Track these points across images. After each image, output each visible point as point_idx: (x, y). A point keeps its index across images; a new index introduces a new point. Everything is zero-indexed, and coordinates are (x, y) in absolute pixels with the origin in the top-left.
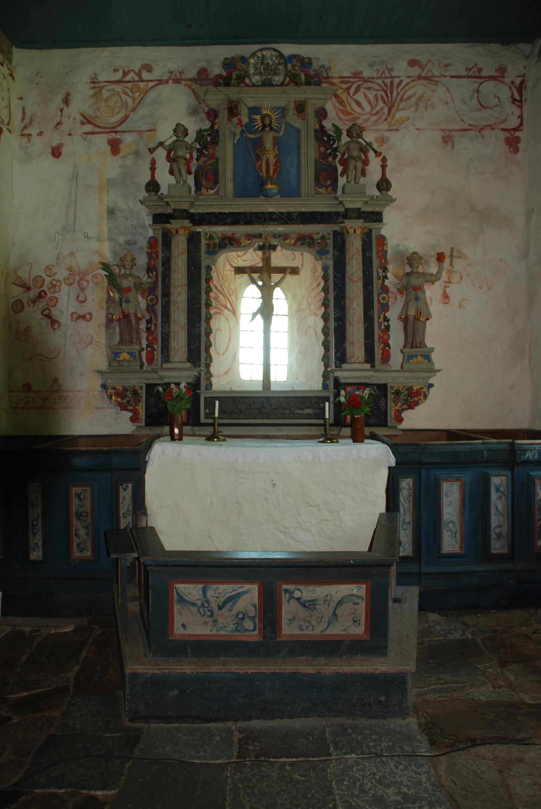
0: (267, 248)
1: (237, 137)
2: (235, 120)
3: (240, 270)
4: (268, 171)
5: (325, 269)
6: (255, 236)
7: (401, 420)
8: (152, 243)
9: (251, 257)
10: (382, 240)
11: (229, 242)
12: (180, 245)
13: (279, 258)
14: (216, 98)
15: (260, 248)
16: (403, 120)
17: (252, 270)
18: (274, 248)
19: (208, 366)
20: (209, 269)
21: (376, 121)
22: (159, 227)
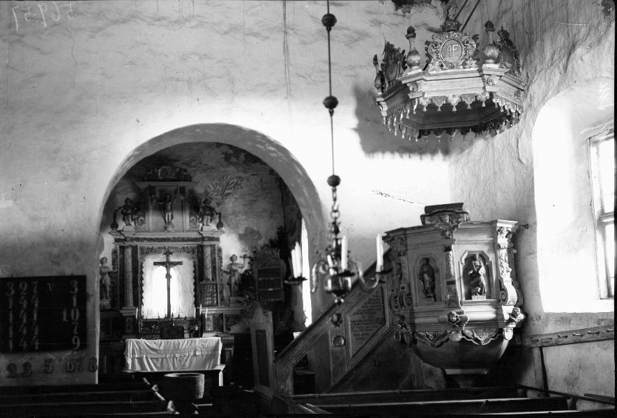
0: (168, 253)
3: (155, 264)
5: (194, 262)
9: (161, 258)
10: (220, 250)
11: (151, 251)
12: (129, 251)
15: (164, 254)
16: (229, 194)
18: (171, 253)
20: (142, 264)
22: (116, 243)
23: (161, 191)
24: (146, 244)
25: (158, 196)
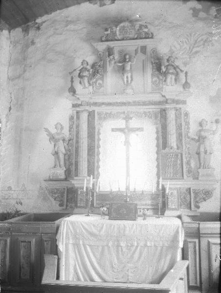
0: (127, 118)
1: (113, 65)
2: (111, 57)
3: (113, 130)
4: (127, 81)
5: (157, 128)
6: (121, 113)
7: (198, 207)
8: (72, 118)
9: (121, 123)
10: (187, 115)
11: (109, 116)
12: (84, 117)
13: (134, 123)
14: (102, 47)
15: (124, 119)
16: (197, 52)
17: (121, 130)
18: (131, 118)
19: (98, 178)
20: (99, 130)
21: (183, 54)
22: (73, 109)
23: (120, 52)
24: (104, 109)
25: (117, 57)
